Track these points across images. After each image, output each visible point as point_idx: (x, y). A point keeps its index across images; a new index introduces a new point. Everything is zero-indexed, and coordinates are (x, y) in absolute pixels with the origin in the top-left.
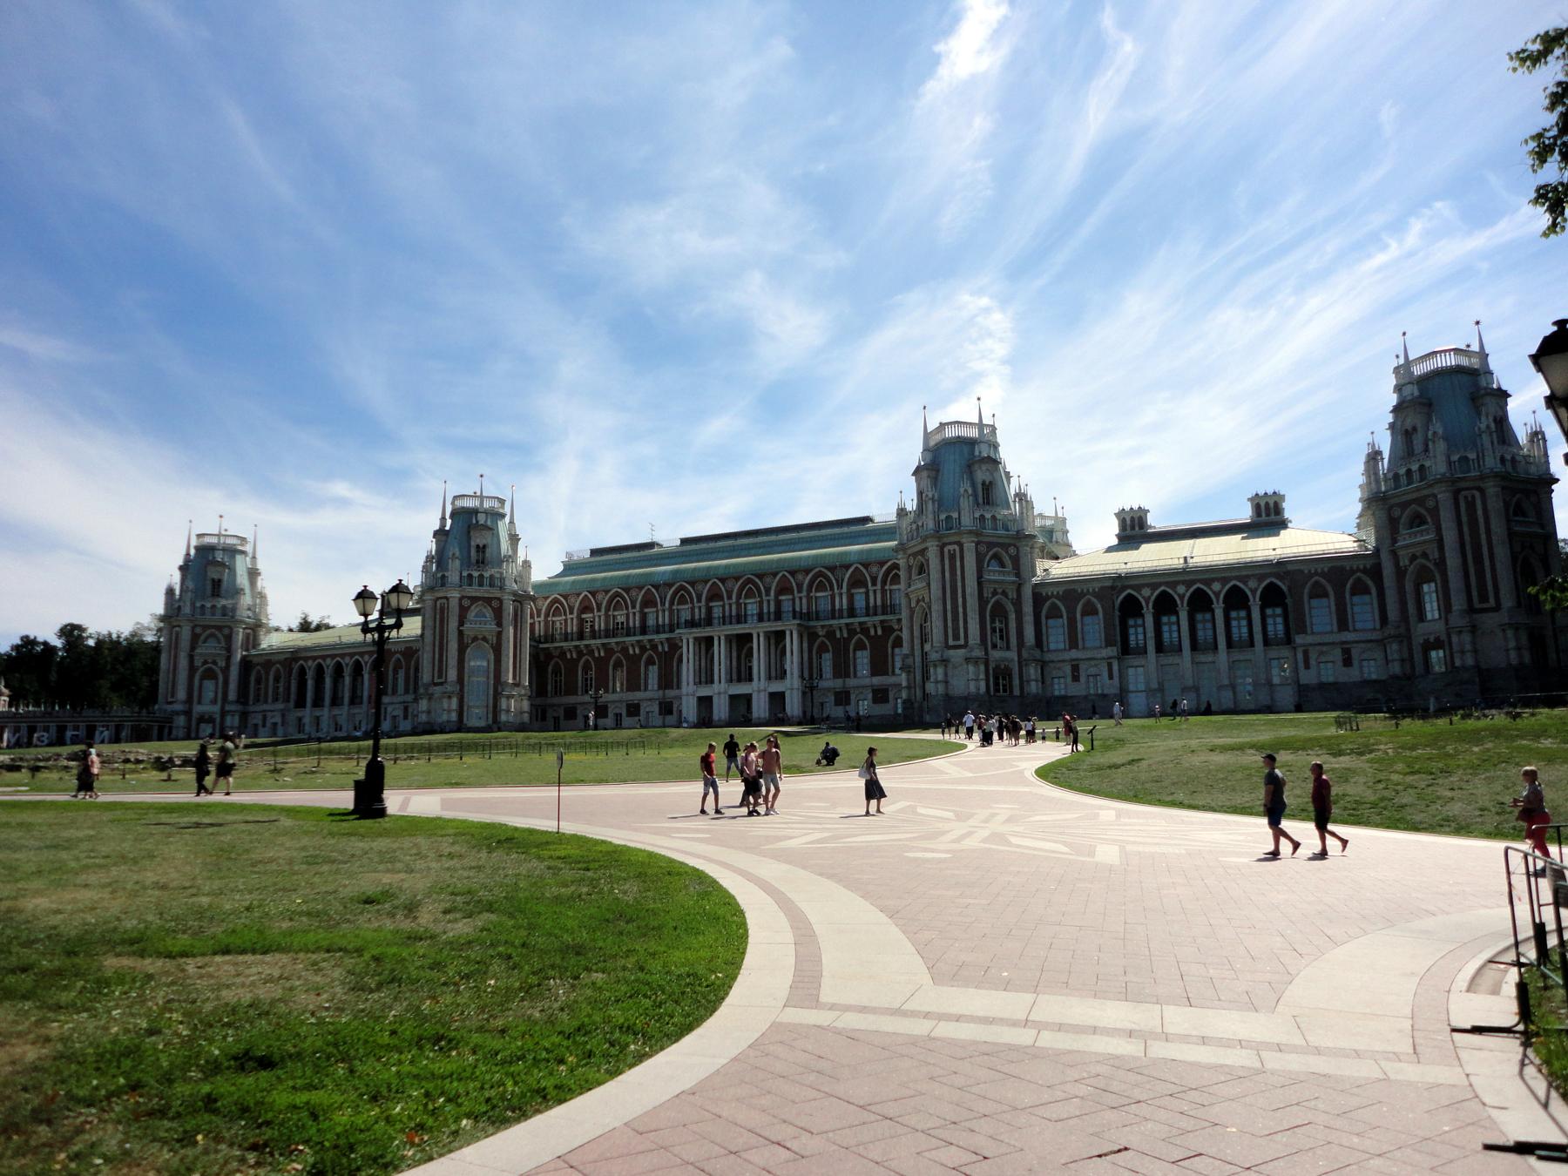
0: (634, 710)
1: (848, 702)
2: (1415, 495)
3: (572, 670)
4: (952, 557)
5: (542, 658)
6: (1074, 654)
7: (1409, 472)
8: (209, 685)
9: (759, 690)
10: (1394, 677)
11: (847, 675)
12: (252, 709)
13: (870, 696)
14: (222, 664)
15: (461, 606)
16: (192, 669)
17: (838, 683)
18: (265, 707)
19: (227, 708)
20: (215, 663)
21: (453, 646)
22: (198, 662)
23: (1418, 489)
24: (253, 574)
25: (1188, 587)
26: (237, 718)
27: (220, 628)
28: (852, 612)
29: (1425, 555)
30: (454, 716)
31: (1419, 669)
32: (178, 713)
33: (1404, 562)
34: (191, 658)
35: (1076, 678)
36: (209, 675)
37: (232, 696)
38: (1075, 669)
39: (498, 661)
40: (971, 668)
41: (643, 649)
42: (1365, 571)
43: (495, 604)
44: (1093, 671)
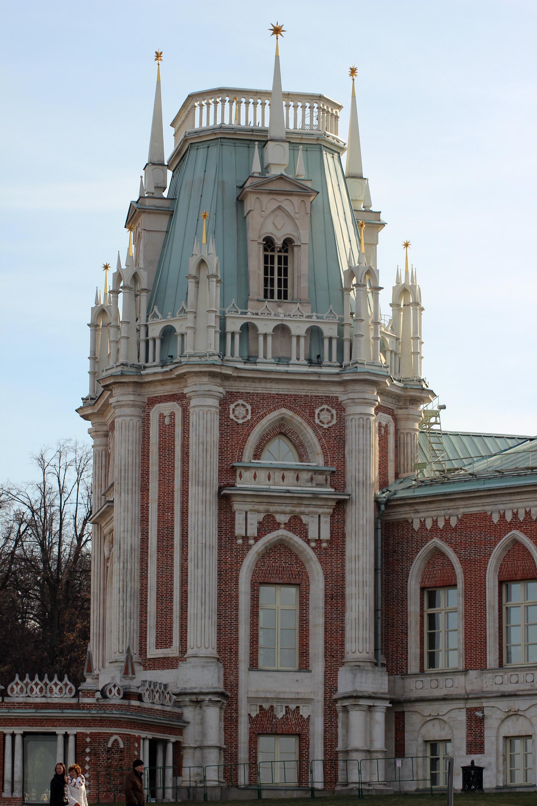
8: (279, 602)
12: (416, 687)
14: (320, 528)
16: (230, 547)
18: (473, 682)
19: (346, 683)
20: (296, 525)
24: (369, 223)
26: (379, 717)
27: (306, 406)
32: (197, 700)
36: (281, 568)
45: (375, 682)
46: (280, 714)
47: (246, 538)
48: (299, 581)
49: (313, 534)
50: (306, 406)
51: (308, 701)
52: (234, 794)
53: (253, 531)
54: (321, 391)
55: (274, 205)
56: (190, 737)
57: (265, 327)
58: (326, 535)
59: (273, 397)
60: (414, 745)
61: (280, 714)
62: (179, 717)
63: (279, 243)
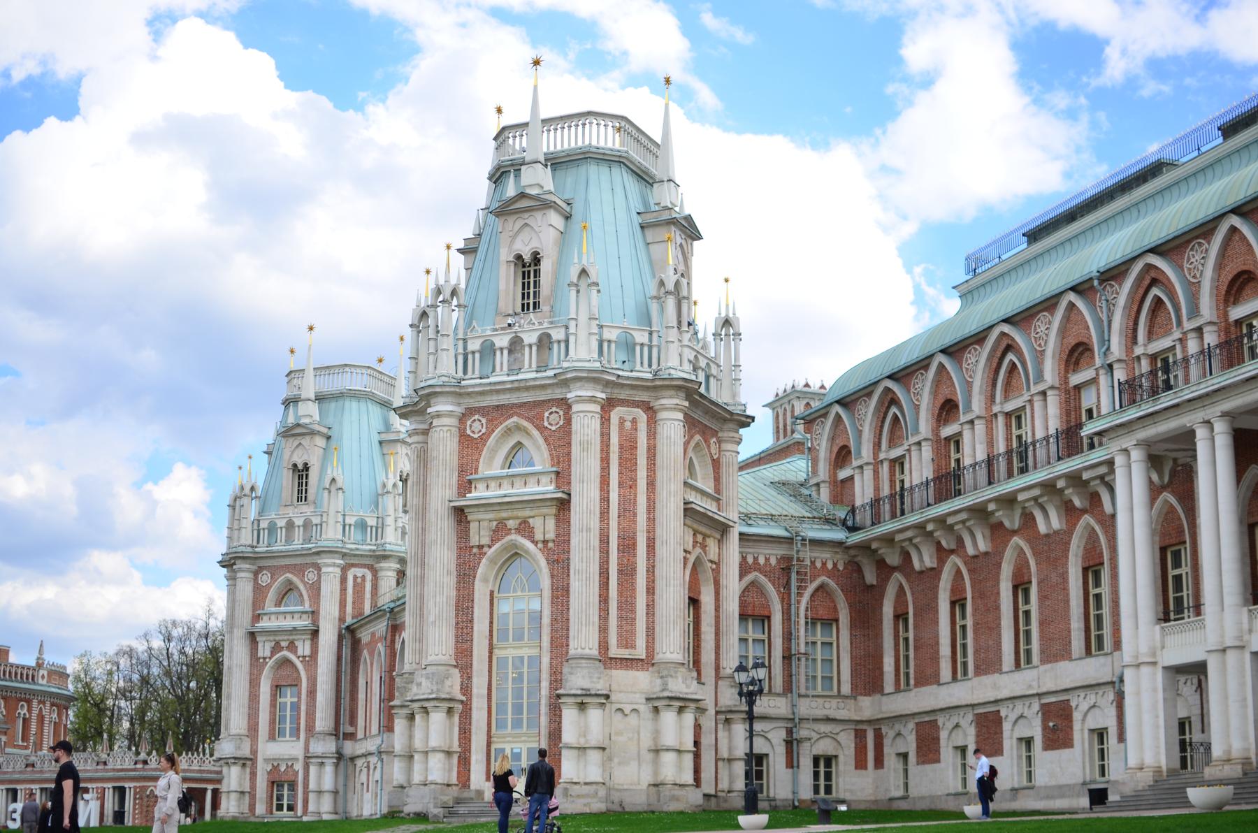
0: (1057, 723)
3: (928, 610)
5: (870, 577)
14: (304, 648)
15: (463, 436)
16: (256, 662)
20: (292, 647)
21: (442, 557)
22: (264, 649)
26: (329, 769)
30: (438, 770)
34: (252, 635)
37: (323, 720)
39: (561, 593)
41: (1070, 511)
43: (553, 419)
45: (329, 746)
46: (283, 768)
47: (264, 658)
48: (296, 684)
49: (300, 652)
50: (300, 570)
51: (297, 759)
52: (252, 819)
53: (268, 654)
54: (309, 560)
55: (296, 443)
56: (223, 788)
57: (281, 523)
58: (307, 652)
59: (282, 567)
60: (358, 786)
61: (283, 768)
62: (220, 772)
63: (300, 467)
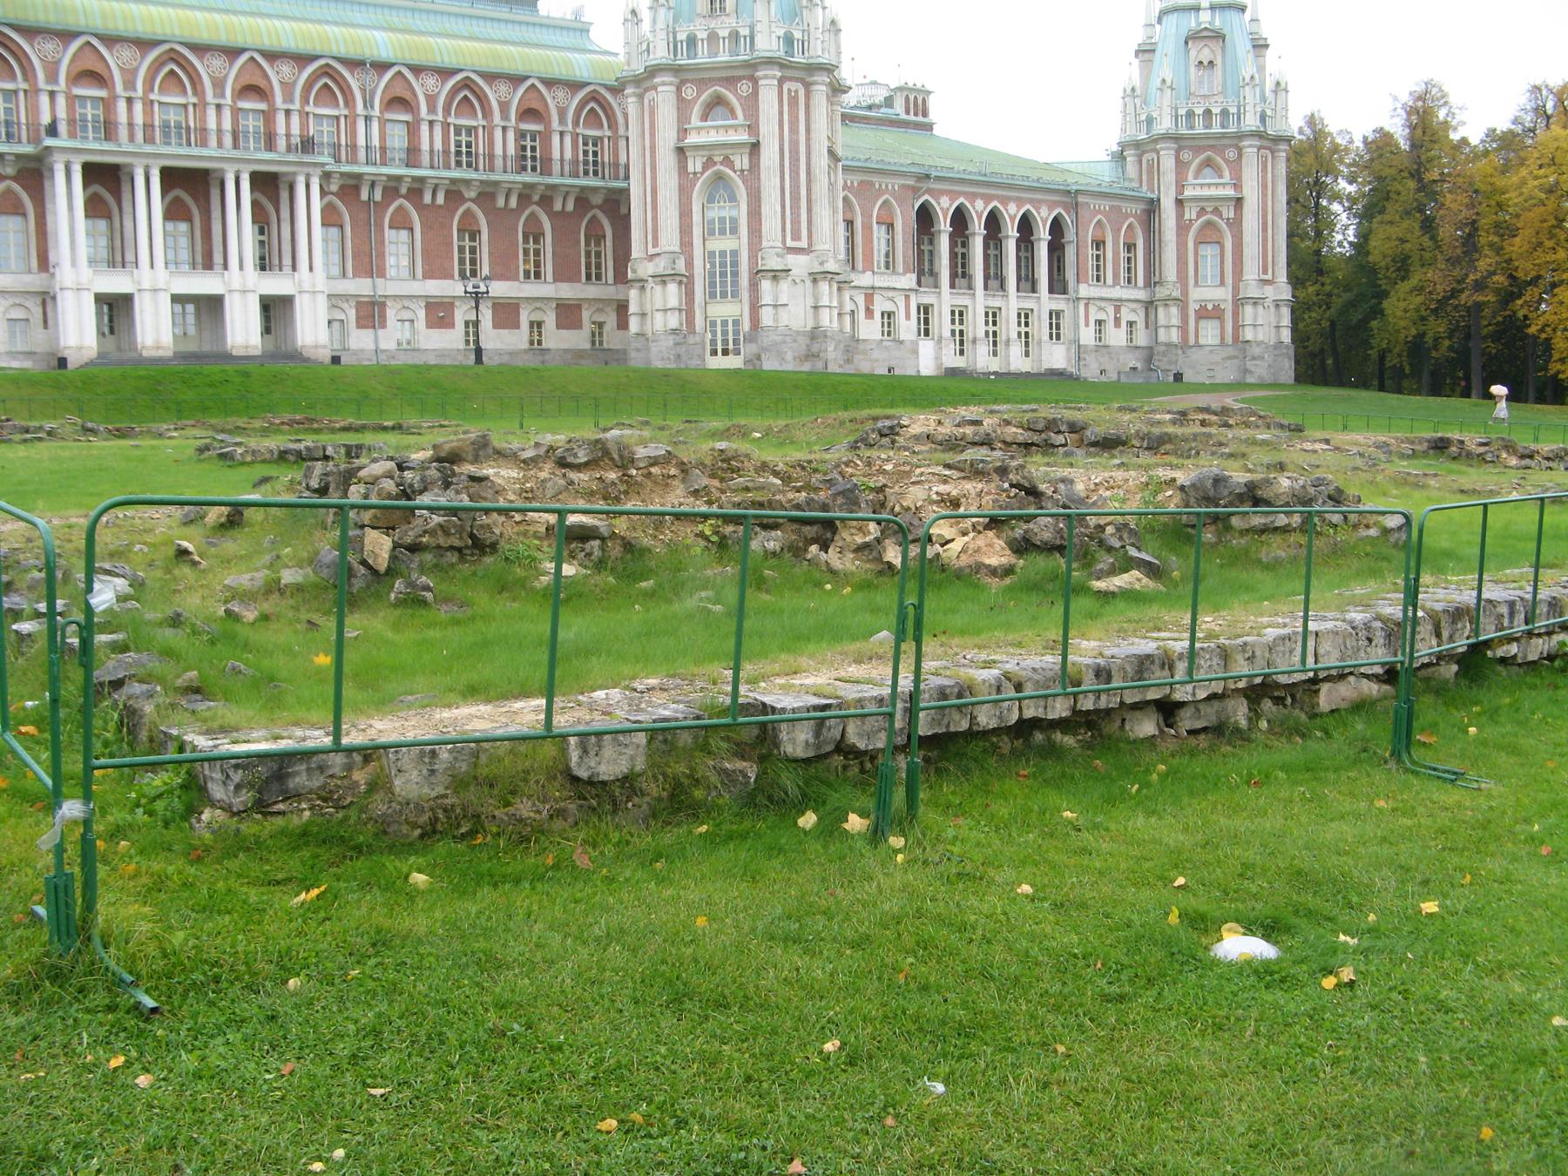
1: (383, 325)
2: (1212, 142)
4: (793, 102)
6: (865, 279)
7: (1208, 112)
9: (241, 288)
10: (1168, 345)
11: (382, 274)
13: (422, 314)
17: (362, 287)
23: (1223, 136)
25: (986, 205)
28: (412, 155)
29: (1216, 211)
31: (1192, 341)
33: (1190, 213)
35: (869, 313)
38: (869, 299)
40: (824, 287)
42: (1135, 216)
44: (889, 307)
